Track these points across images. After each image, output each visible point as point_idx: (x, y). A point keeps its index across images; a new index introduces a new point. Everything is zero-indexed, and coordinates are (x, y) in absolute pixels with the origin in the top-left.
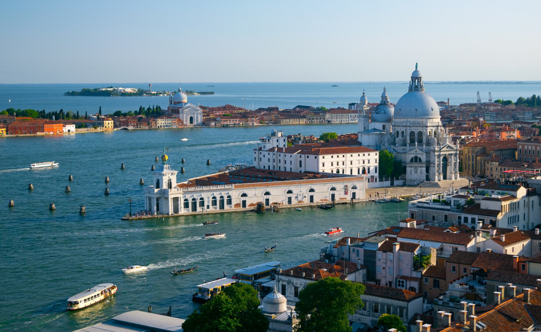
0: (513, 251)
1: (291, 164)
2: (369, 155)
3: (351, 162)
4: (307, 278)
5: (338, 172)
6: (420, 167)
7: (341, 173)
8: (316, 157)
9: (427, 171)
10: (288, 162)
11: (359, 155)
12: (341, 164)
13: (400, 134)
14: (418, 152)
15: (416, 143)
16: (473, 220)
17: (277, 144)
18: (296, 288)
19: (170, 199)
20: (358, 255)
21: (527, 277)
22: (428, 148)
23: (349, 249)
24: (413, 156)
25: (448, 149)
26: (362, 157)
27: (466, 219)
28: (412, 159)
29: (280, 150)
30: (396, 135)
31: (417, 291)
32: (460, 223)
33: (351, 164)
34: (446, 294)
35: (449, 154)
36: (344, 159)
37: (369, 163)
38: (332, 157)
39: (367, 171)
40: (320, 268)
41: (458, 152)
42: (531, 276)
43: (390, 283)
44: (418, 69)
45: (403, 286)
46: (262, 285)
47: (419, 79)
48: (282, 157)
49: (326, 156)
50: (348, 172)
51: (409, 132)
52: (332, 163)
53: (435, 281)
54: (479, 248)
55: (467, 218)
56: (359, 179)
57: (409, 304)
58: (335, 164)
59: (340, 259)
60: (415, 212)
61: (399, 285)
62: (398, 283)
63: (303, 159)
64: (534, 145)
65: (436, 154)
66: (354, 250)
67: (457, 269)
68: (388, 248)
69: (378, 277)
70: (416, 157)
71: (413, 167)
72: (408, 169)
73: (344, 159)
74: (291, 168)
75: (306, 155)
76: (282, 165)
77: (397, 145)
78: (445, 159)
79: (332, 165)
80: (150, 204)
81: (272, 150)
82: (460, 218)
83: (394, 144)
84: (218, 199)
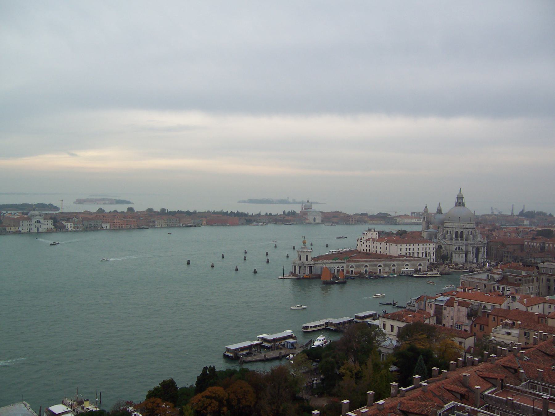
0: (532, 310)
1: (380, 249)
2: (429, 245)
3: (418, 249)
4: (400, 320)
5: (410, 254)
6: (462, 253)
7: (411, 255)
8: (396, 245)
9: (466, 256)
10: (379, 248)
11: (423, 245)
12: (411, 249)
13: (449, 233)
14: (460, 244)
15: (459, 239)
16: (503, 289)
17: (372, 236)
18: (392, 327)
19: (307, 267)
20: (431, 308)
21: (547, 328)
22: (466, 242)
23: (425, 303)
24: (457, 246)
25: (480, 243)
26: (425, 246)
27: (498, 288)
28: (456, 249)
29: (373, 240)
30: (446, 233)
31: (469, 332)
32: (494, 290)
33: (418, 250)
34: (490, 335)
35: (480, 246)
36: (414, 247)
37: (429, 250)
38: (406, 245)
39: (427, 255)
40: (407, 314)
41: (486, 245)
42: (550, 327)
43: (451, 326)
44: (461, 192)
45: (460, 328)
46: (369, 323)
47: (462, 198)
48: (375, 245)
49: (402, 245)
50: (416, 255)
51: (455, 231)
52: (406, 249)
53: (481, 326)
54: (509, 307)
55: (499, 287)
56: (424, 260)
57: (466, 340)
58: (408, 250)
59: (419, 309)
60: (464, 282)
61: (457, 328)
62: (457, 326)
63: (388, 246)
64: (551, 244)
65: (472, 245)
66: (428, 304)
67: (496, 319)
68: (450, 303)
69: (444, 322)
70: (459, 247)
71: (457, 253)
72: (453, 255)
73: (414, 247)
74: (380, 252)
75: (390, 244)
76: (375, 249)
77: (447, 239)
78: (478, 249)
79: (406, 250)
80: (295, 270)
81: (369, 240)
82: (494, 287)
83: (445, 239)
84: (336, 268)
